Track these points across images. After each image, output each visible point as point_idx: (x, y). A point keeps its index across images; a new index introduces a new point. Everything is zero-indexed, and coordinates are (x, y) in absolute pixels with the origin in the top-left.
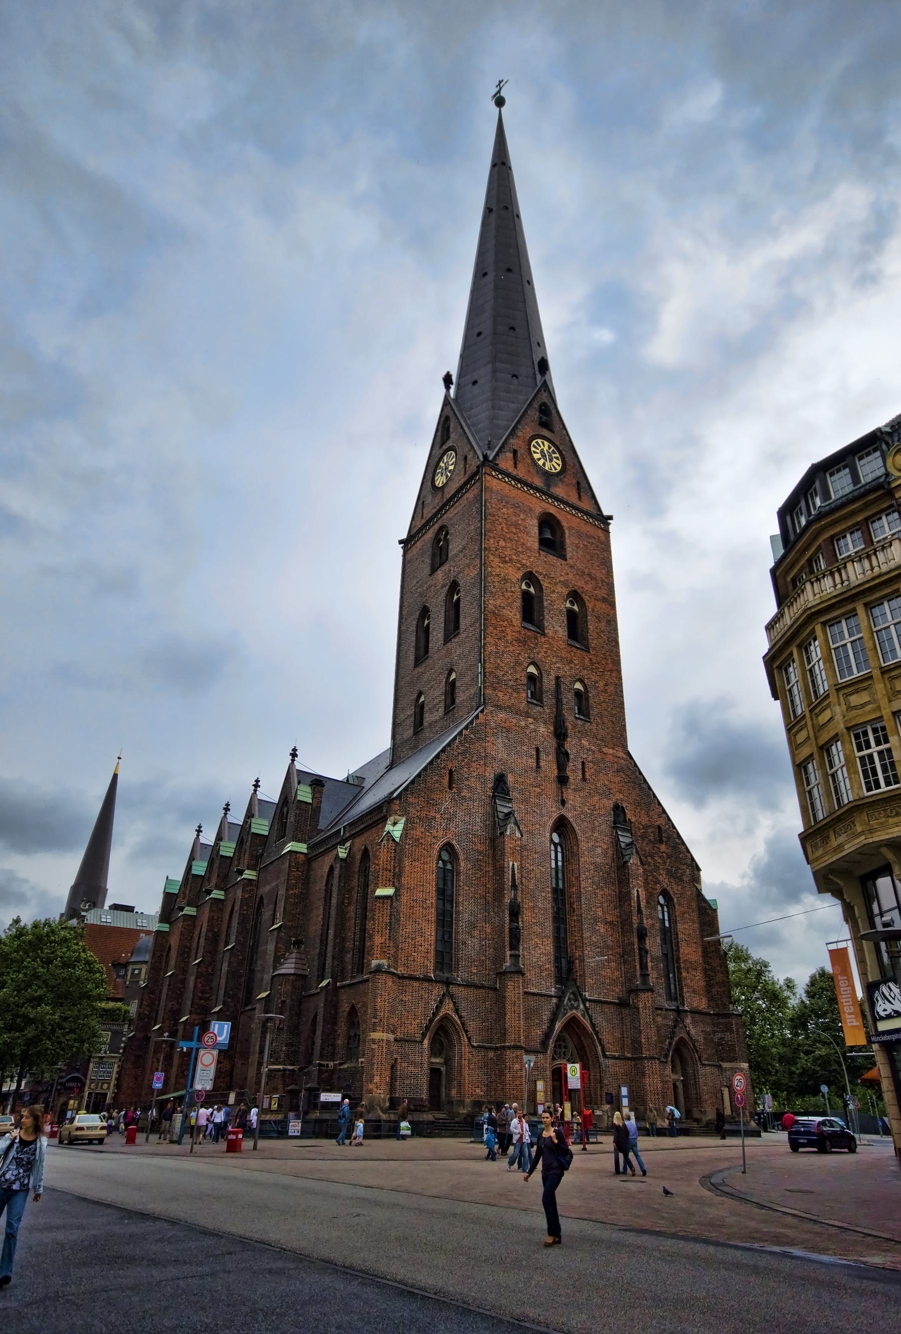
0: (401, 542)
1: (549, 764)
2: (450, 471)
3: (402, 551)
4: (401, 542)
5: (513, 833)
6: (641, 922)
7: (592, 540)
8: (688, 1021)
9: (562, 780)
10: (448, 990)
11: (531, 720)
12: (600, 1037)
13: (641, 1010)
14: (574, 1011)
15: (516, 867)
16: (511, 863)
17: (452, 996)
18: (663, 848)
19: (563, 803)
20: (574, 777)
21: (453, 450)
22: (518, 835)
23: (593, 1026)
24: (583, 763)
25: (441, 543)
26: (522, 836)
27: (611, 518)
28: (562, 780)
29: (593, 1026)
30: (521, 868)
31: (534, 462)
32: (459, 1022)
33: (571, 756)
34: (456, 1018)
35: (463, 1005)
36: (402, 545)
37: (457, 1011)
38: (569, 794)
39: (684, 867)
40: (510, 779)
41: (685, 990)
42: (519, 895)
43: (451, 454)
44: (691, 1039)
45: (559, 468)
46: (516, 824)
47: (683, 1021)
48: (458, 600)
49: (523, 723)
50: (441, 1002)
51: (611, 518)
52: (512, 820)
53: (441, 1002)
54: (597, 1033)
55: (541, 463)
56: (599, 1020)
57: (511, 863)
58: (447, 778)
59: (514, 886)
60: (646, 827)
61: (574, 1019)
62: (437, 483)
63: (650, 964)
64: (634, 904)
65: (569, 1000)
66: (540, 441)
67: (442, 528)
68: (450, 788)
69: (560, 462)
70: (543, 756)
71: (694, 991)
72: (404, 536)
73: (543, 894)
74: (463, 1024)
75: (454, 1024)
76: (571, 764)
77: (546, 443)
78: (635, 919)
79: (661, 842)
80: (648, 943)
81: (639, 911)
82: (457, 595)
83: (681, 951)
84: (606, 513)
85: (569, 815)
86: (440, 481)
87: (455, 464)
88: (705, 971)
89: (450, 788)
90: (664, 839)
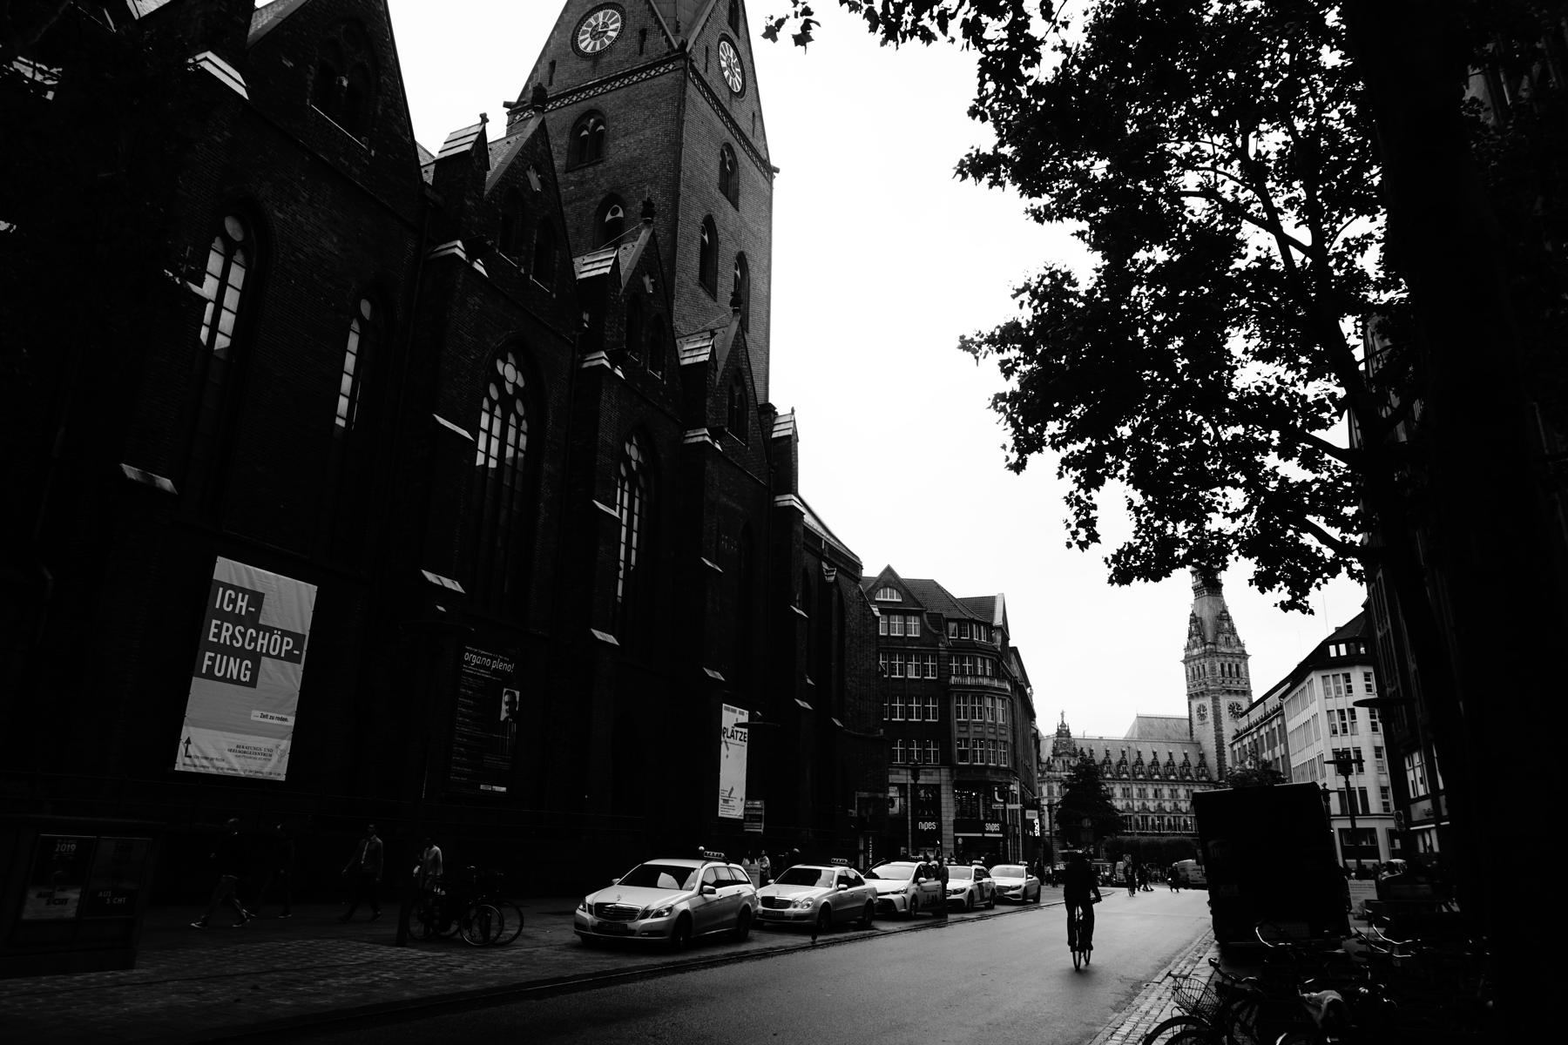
0: (506, 105)
2: (609, 38)
3: (506, 119)
4: (506, 105)
25: (585, 133)
27: (777, 171)
31: (722, 70)
36: (509, 110)
43: (614, 15)
45: (739, 88)
51: (777, 171)
55: (726, 73)
62: (582, 46)
66: (727, 44)
67: (591, 113)
69: (740, 81)
72: (514, 99)
77: (732, 51)
82: (612, 214)
84: (774, 162)
86: (586, 44)
87: (622, 31)
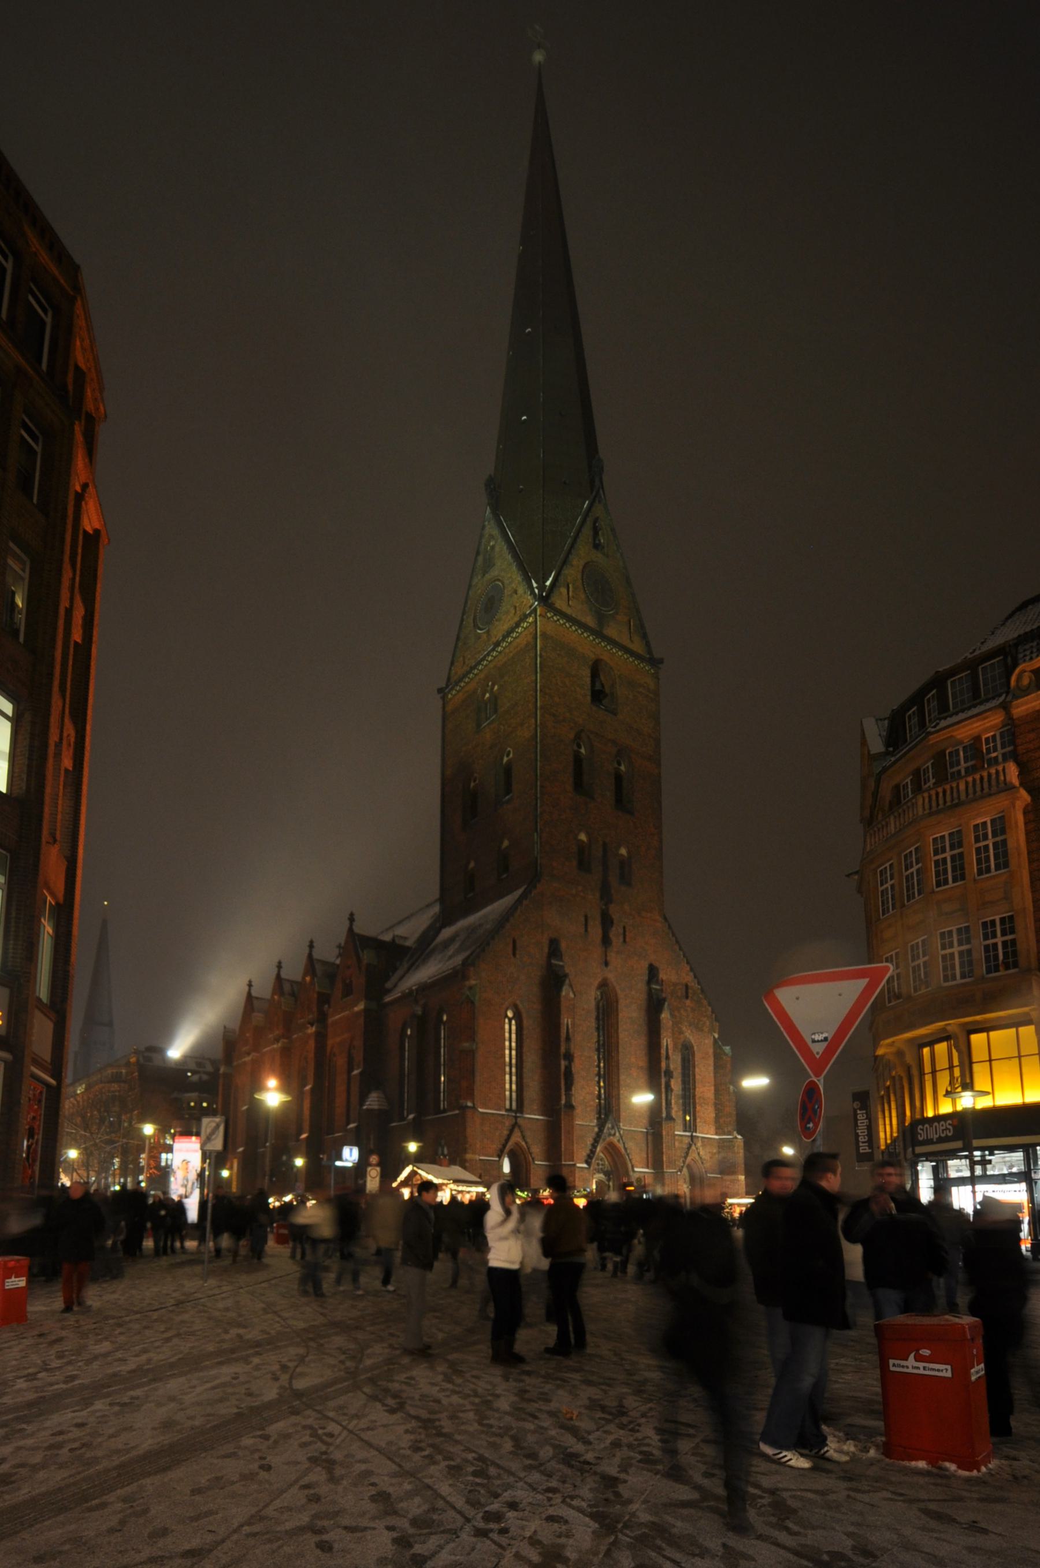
1: (596, 931)
5: (568, 994)
6: (668, 1066)
7: (641, 690)
8: (699, 1144)
9: (606, 941)
10: (516, 1123)
11: (580, 888)
12: (631, 1157)
13: (664, 1136)
14: (612, 1137)
15: (570, 1023)
16: (566, 1020)
17: (519, 1127)
18: (688, 1002)
19: (606, 964)
20: (616, 940)
21: (499, 580)
22: (572, 995)
23: (626, 1149)
24: (624, 928)
26: (575, 995)
28: (606, 941)
29: (626, 1149)
30: (573, 1024)
32: (525, 1146)
33: (615, 921)
34: (523, 1143)
35: (528, 1134)
37: (524, 1138)
38: (612, 956)
39: (705, 1019)
40: (563, 945)
41: (698, 1120)
42: (572, 1046)
44: (701, 1158)
46: (571, 986)
47: (695, 1145)
48: (509, 762)
49: (574, 892)
50: (511, 1131)
52: (567, 982)
53: (511, 1131)
54: (628, 1155)
56: (630, 1145)
57: (566, 1020)
58: (511, 946)
59: (568, 1039)
60: (675, 985)
61: (611, 1145)
63: (673, 1101)
64: (663, 1052)
65: (608, 1129)
68: (514, 954)
70: (591, 923)
71: (705, 1122)
73: (589, 1045)
74: (528, 1148)
75: (521, 1148)
76: (614, 929)
78: (663, 1065)
79: (687, 997)
80: (673, 1082)
81: (667, 1057)
83: (697, 1089)
85: (611, 977)
88: (716, 1105)
89: (514, 954)
90: (690, 995)
